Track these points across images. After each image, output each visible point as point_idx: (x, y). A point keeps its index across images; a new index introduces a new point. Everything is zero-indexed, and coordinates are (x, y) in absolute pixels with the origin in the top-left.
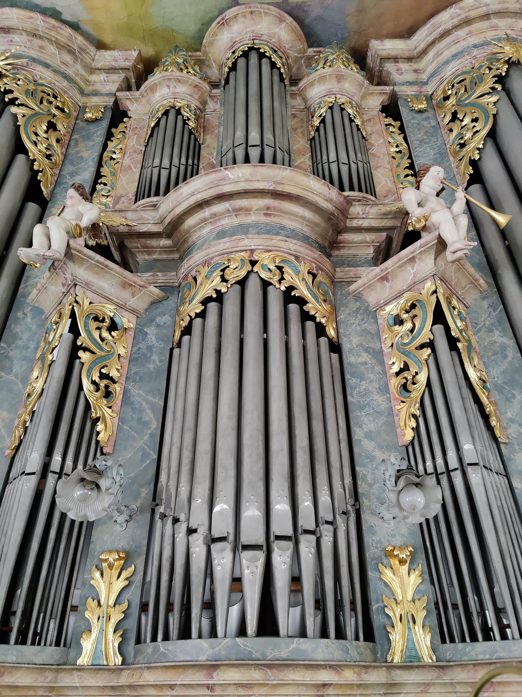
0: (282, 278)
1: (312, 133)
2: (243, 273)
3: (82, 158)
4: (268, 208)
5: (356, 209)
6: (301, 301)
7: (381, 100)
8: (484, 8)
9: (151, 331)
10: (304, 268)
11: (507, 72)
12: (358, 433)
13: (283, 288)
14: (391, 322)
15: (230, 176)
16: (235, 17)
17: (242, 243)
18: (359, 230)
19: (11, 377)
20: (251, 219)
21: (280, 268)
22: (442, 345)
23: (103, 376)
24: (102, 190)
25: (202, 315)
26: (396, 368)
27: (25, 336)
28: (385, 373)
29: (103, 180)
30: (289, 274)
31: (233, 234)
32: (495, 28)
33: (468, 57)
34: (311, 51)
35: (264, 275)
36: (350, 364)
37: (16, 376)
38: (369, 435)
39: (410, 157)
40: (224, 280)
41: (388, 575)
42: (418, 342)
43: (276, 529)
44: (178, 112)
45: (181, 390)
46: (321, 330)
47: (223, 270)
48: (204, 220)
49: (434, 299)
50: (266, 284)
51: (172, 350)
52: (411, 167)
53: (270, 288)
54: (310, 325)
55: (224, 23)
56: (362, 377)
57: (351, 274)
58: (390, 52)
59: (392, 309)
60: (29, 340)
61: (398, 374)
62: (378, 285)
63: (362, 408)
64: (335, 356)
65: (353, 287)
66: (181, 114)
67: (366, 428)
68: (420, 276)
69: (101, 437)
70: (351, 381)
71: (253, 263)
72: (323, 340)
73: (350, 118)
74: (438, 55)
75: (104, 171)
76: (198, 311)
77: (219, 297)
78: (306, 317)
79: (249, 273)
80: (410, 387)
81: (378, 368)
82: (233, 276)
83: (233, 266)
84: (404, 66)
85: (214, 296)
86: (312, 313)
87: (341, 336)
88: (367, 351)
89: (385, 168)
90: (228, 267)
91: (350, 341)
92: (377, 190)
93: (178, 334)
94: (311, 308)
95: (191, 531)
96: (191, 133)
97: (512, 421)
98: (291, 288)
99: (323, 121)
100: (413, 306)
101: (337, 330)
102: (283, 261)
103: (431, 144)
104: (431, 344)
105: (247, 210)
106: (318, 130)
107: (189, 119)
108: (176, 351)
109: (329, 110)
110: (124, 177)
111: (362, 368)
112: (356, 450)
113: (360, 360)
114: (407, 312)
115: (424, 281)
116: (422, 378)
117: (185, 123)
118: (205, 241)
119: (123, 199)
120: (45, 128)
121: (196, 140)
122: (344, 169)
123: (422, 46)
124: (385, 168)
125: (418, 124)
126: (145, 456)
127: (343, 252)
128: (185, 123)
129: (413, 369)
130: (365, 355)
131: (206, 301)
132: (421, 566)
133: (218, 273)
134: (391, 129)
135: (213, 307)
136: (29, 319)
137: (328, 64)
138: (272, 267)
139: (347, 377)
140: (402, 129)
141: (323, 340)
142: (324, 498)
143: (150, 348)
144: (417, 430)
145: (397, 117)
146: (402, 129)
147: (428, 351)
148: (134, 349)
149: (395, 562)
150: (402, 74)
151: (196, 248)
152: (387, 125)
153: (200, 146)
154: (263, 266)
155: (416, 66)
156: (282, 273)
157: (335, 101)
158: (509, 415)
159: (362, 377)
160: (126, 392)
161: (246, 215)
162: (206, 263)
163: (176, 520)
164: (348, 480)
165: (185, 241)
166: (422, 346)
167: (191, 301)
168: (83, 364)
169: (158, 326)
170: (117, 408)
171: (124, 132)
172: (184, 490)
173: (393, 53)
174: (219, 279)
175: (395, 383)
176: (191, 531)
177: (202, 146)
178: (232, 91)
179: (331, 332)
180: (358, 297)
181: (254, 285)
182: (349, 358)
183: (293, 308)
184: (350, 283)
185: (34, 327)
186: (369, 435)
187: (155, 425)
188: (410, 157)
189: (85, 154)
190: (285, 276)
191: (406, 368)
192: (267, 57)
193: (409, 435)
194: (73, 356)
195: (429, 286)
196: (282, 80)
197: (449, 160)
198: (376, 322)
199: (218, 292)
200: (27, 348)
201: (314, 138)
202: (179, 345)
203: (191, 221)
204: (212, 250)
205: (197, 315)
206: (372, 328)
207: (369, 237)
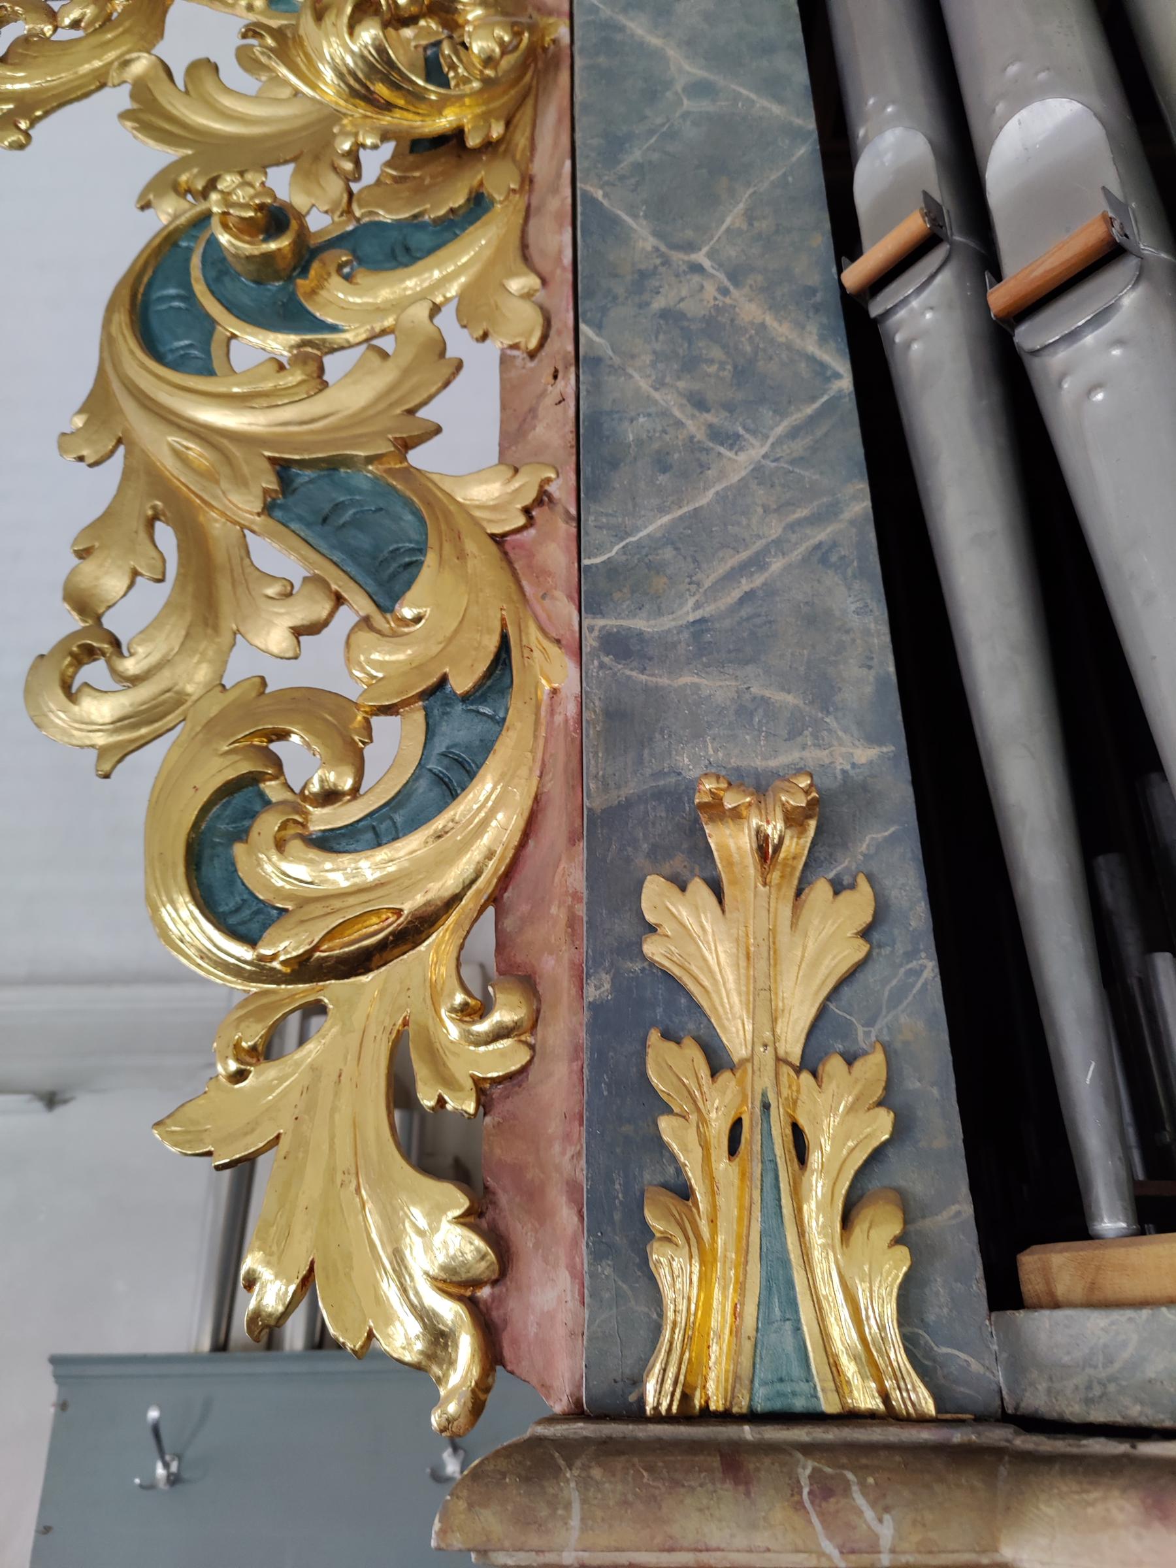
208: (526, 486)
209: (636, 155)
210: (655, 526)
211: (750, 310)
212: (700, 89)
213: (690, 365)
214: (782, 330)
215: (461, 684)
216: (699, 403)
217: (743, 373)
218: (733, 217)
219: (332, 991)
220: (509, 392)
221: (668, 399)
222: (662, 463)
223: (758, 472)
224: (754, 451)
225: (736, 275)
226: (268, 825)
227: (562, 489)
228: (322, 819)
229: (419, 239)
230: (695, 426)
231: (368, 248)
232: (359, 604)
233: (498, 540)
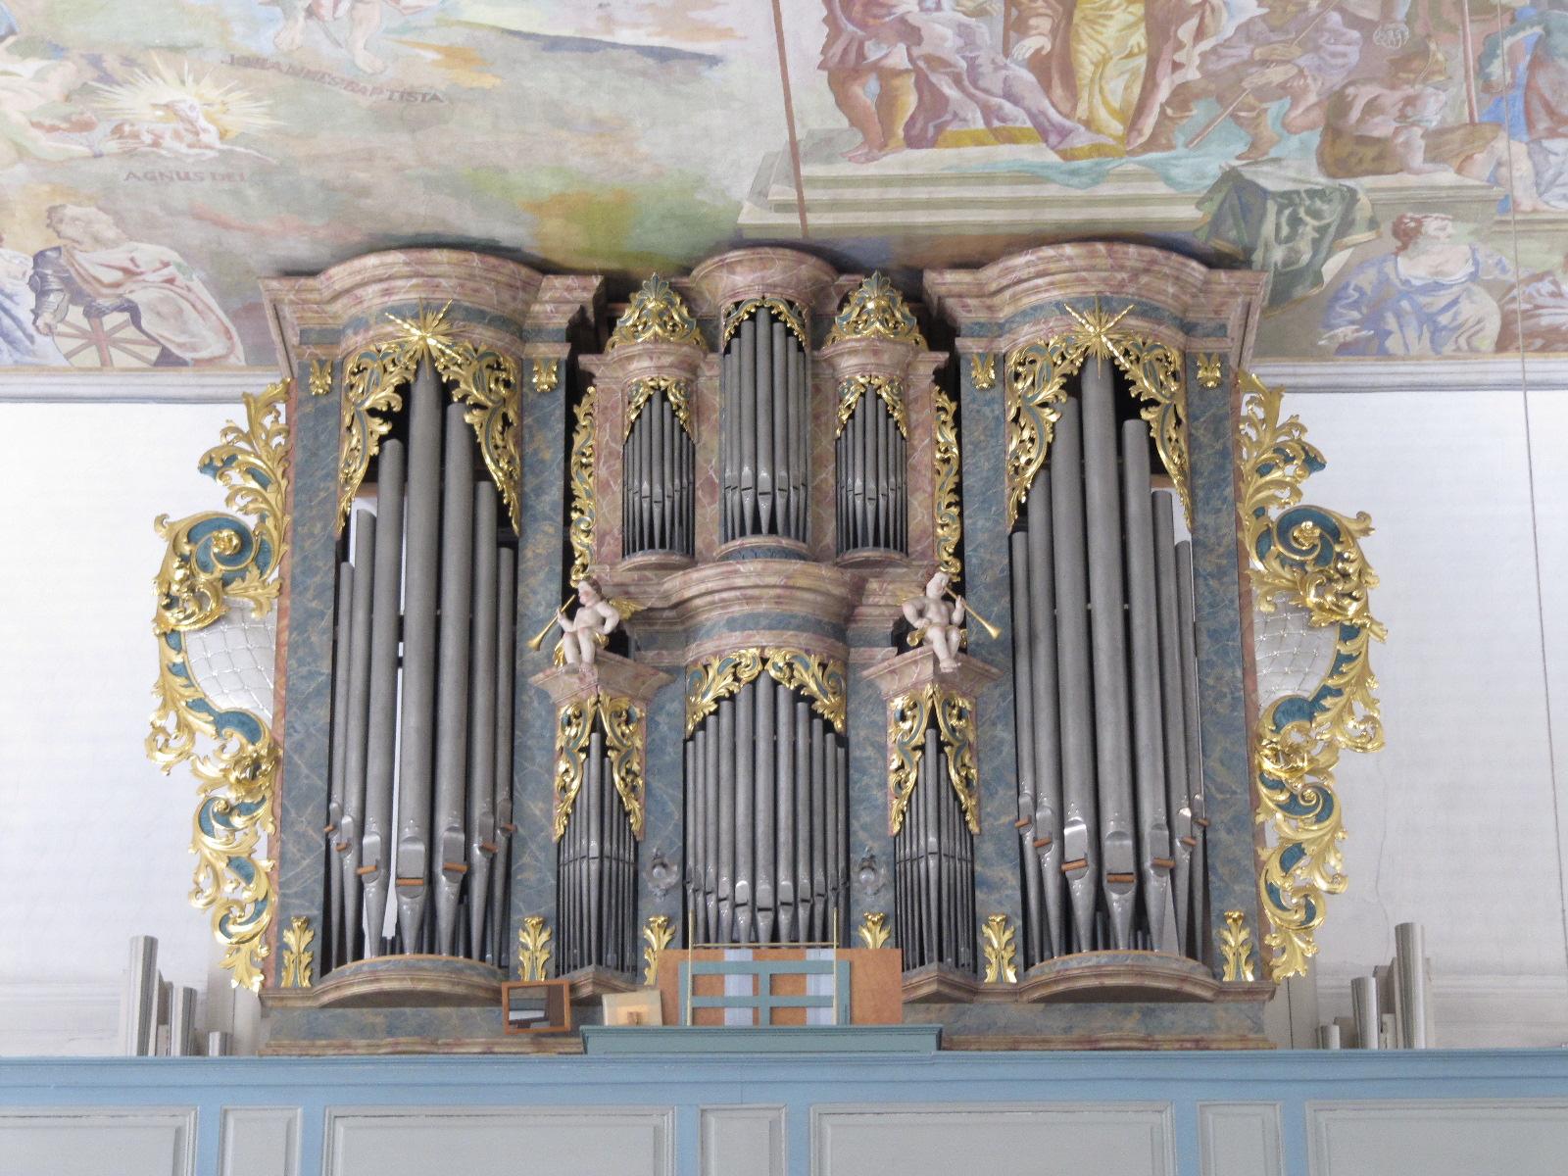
0: (792, 677)
1: (838, 432)
2: (756, 672)
3: (542, 461)
4: (779, 597)
5: (873, 585)
6: (811, 700)
7: (935, 366)
8: (1067, 263)
9: (662, 719)
10: (814, 661)
11: (1082, 369)
12: (855, 825)
13: (792, 687)
14: (898, 715)
15: (742, 569)
16: (740, 262)
17: (753, 639)
18: (876, 605)
19: (536, 768)
20: (762, 607)
21: (790, 665)
22: (931, 749)
23: (629, 771)
24: (580, 521)
25: (716, 713)
26: (895, 765)
27: (538, 723)
28: (886, 768)
29: (577, 503)
30: (799, 671)
31: (744, 627)
32: (1084, 281)
33: (1043, 326)
34: (843, 280)
35: (773, 673)
36: (855, 759)
37: (541, 767)
38: (864, 827)
39: (960, 473)
40: (736, 679)
41: (865, 932)
42: (914, 743)
43: (782, 897)
44: (664, 396)
45: (700, 786)
46: (828, 726)
47: (735, 666)
48: (713, 603)
49: (929, 704)
50: (775, 684)
51: (685, 742)
52: (958, 490)
53: (780, 687)
54: (817, 724)
55: (723, 265)
56: (864, 772)
57: (866, 655)
58: (952, 287)
59: (899, 703)
60: (543, 727)
61: (897, 770)
62: (889, 677)
63: (861, 802)
64: (841, 751)
65: (865, 673)
66: (668, 400)
67: (862, 821)
68: (922, 677)
69: (634, 828)
70: (854, 775)
71: (764, 661)
72: (830, 736)
73: (888, 411)
74: (1015, 298)
75: (578, 486)
76: (712, 709)
77: (732, 697)
78: (813, 714)
79: (760, 673)
80: (903, 785)
81: (880, 763)
82: (746, 675)
83: (744, 662)
84: (969, 301)
85: (727, 695)
86: (820, 711)
87: (850, 728)
88: (872, 745)
89: (924, 491)
90: (740, 663)
91: (858, 734)
92: (910, 529)
93: (690, 727)
94: (818, 706)
95: (719, 900)
96: (682, 429)
97: (989, 814)
98: (801, 687)
99: (852, 417)
100: (915, 705)
101: (845, 723)
102: (794, 657)
103: (988, 451)
104: (922, 748)
105: (757, 599)
106: (845, 428)
107: (679, 407)
108: (690, 744)
109: (862, 398)
110: (603, 498)
111: (865, 763)
112: (852, 840)
113: (865, 754)
114: (911, 709)
115: (924, 682)
116: (912, 777)
117: (673, 415)
118: (714, 626)
119: (608, 538)
120: (500, 428)
121: (689, 439)
122: (870, 507)
123: (994, 286)
124: (924, 491)
125: (978, 411)
126: (672, 843)
127: (860, 625)
128: (673, 415)
129: (907, 768)
130: (870, 749)
131: (718, 700)
132: (891, 926)
133: (729, 670)
134: (943, 417)
135: (725, 705)
136: (536, 704)
137: (864, 318)
138: (781, 664)
139: (851, 772)
140: (957, 418)
141: (830, 736)
142: (819, 876)
143: (663, 739)
144: (902, 824)
145: (955, 395)
146: (957, 418)
147: (919, 754)
148: (649, 740)
149: (870, 924)
150: (970, 311)
151: (703, 632)
152: (939, 409)
153: (694, 445)
154: (775, 665)
155: (988, 301)
156: (792, 670)
157: (870, 382)
158: (989, 810)
159: (864, 772)
160: (646, 784)
161: (757, 603)
162: (715, 654)
163: (706, 894)
164: (842, 864)
165: (692, 617)
166: (915, 748)
167: (704, 695)
168: (612, 764)
169: (669, 714)
170: (641, 800)
171: (590, 414)
172: (711, 870)
173: (956, 289)
174: (730, 679)
175: (893, 779)
176: (719, 900)
177: (697, 447)
178: (735, 360)
179: (838, 725)
180: (871, 684)
181: (763, 687)
182: (855, 753)
183: (801, 705)
184: (866, 666)
185: (543, 713)
186: (864, 827)
187: (678, 816)
188: (960, 473)
189: (547, 455)
190: (795, 673)
191: (902, 767)
192: (780, 321)
193: (896, 828)
194: (603, 753)
195: (929, 690)
196: (800, 348)
197: (1003, 482)
198: (885, 713)
199: (731, 693)
200: (542, 736)
201: (839, 438)
202: (692, 737)
203: (698, 602)
204: (724, 642)
205: (711, 713)
206: (879, 719)
207: (887, 611)
208: (271, 863)
209: (293, 794)
210: (291, 874)
211: (311, 832)
212: (307, 777)
213: (299, 843)
214: (315, 836)
215: (260, 899)
216: (299, 850)
217: (308, 845)
218: (310, 809)
219: (242, 946)
220: (269, 842)
221: (295, 850)
222: (293, 863)
223: (308, 866)
224: (305, 863)
225: (309, 823)
226: (231, 921)
227: (277, 864)
228: (239, 920)
229: (253, 807)
230: (298, 855)
231: (243, 808)
232: (243, 884)
233: (267, 873)
